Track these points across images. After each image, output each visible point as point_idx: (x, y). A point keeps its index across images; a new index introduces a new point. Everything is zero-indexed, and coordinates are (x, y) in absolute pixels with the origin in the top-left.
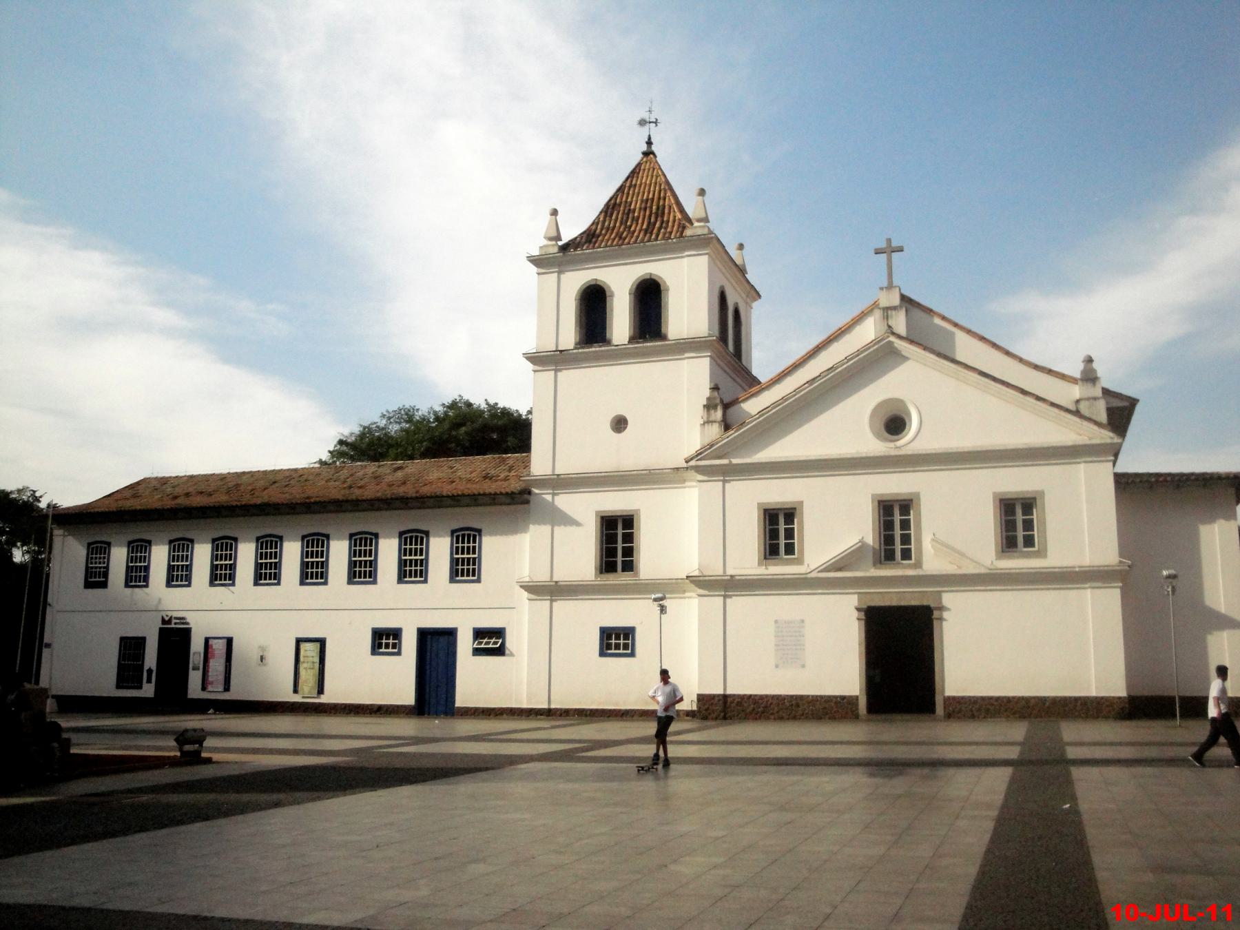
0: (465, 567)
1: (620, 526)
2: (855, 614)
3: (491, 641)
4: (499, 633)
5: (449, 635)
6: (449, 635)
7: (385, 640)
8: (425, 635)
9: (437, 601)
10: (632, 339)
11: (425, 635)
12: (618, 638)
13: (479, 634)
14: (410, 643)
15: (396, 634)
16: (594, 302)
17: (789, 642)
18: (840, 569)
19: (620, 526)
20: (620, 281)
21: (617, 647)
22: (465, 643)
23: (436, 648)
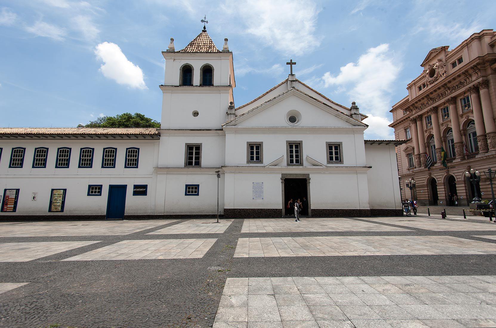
0: (132, 161)
1: (194, 149)
2: (281, 181)
3: (141, 190)
4: (145, 187)
5: (124, 187)
6: (124, 187)
7: (94, 190)
8: (112, 188)
9: (120, 175)
10: (201, 85)
11: (112, 188)
12: (192, 188)
13: (136, 187)
14: (105, 191)
15: (100, 187)
16: (187, 72)
17: (258, 189)
18: (276, 165)
19: (194, 149)
20: (197, 67)
21: (192, 192)
22: (130, 191)
23: (117, 193)
